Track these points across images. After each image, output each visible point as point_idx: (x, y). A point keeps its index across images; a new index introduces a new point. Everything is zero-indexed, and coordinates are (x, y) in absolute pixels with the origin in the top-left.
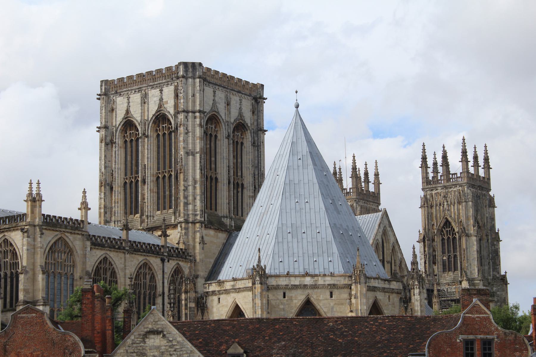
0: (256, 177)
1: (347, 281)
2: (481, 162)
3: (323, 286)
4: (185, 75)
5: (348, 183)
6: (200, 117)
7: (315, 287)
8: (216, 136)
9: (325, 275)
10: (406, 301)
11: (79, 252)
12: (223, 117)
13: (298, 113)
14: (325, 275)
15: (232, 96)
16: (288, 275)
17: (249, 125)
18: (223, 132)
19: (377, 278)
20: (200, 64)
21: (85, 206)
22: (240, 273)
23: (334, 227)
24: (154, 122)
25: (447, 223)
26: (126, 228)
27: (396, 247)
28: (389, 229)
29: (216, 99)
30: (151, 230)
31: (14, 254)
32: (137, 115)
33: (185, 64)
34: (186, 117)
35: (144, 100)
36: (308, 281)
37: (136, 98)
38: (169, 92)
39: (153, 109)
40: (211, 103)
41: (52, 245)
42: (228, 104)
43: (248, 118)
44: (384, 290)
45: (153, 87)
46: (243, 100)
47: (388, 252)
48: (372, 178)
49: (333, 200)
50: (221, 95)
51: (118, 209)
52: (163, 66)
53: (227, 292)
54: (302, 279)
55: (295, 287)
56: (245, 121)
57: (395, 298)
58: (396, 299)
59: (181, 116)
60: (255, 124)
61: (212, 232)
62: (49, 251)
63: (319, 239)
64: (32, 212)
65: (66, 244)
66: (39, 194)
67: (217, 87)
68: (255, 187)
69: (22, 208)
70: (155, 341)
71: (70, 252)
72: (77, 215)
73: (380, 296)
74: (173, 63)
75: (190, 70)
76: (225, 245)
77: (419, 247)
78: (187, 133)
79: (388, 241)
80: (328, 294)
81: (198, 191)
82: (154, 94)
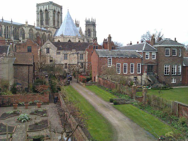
1: (75, 37)
2: (94, 20)
5: (75, 22)
7: (70, 38)
10: (84, 40)
13: (68, 11)
18: (56, 13)
21: (35, 24)
22: (59, 35)
23: (73, 29)
25: (89, 29)
26: (41, 27)
30: (45, 28)
31: (24, 31)
32: (42, 9)
36: (70, 37)
37: (42, 7)
38: (47, 6)
39: (45, 9)
44: (81, 39)
47: (81, 33)
48: (78, 22)
50: (56, 7)
51: (40, 24)
52: (47, 2)
53: (57, 38)
57: (82, 40)
59: (50, 10)
61: (54, 29)
65: (32, 30)
69: (25, 23)
70: (48, 45)
72: (33, 25)
73: (80, 40)
74: (48, 2)
77: (85, 33)
81: (52, 22)
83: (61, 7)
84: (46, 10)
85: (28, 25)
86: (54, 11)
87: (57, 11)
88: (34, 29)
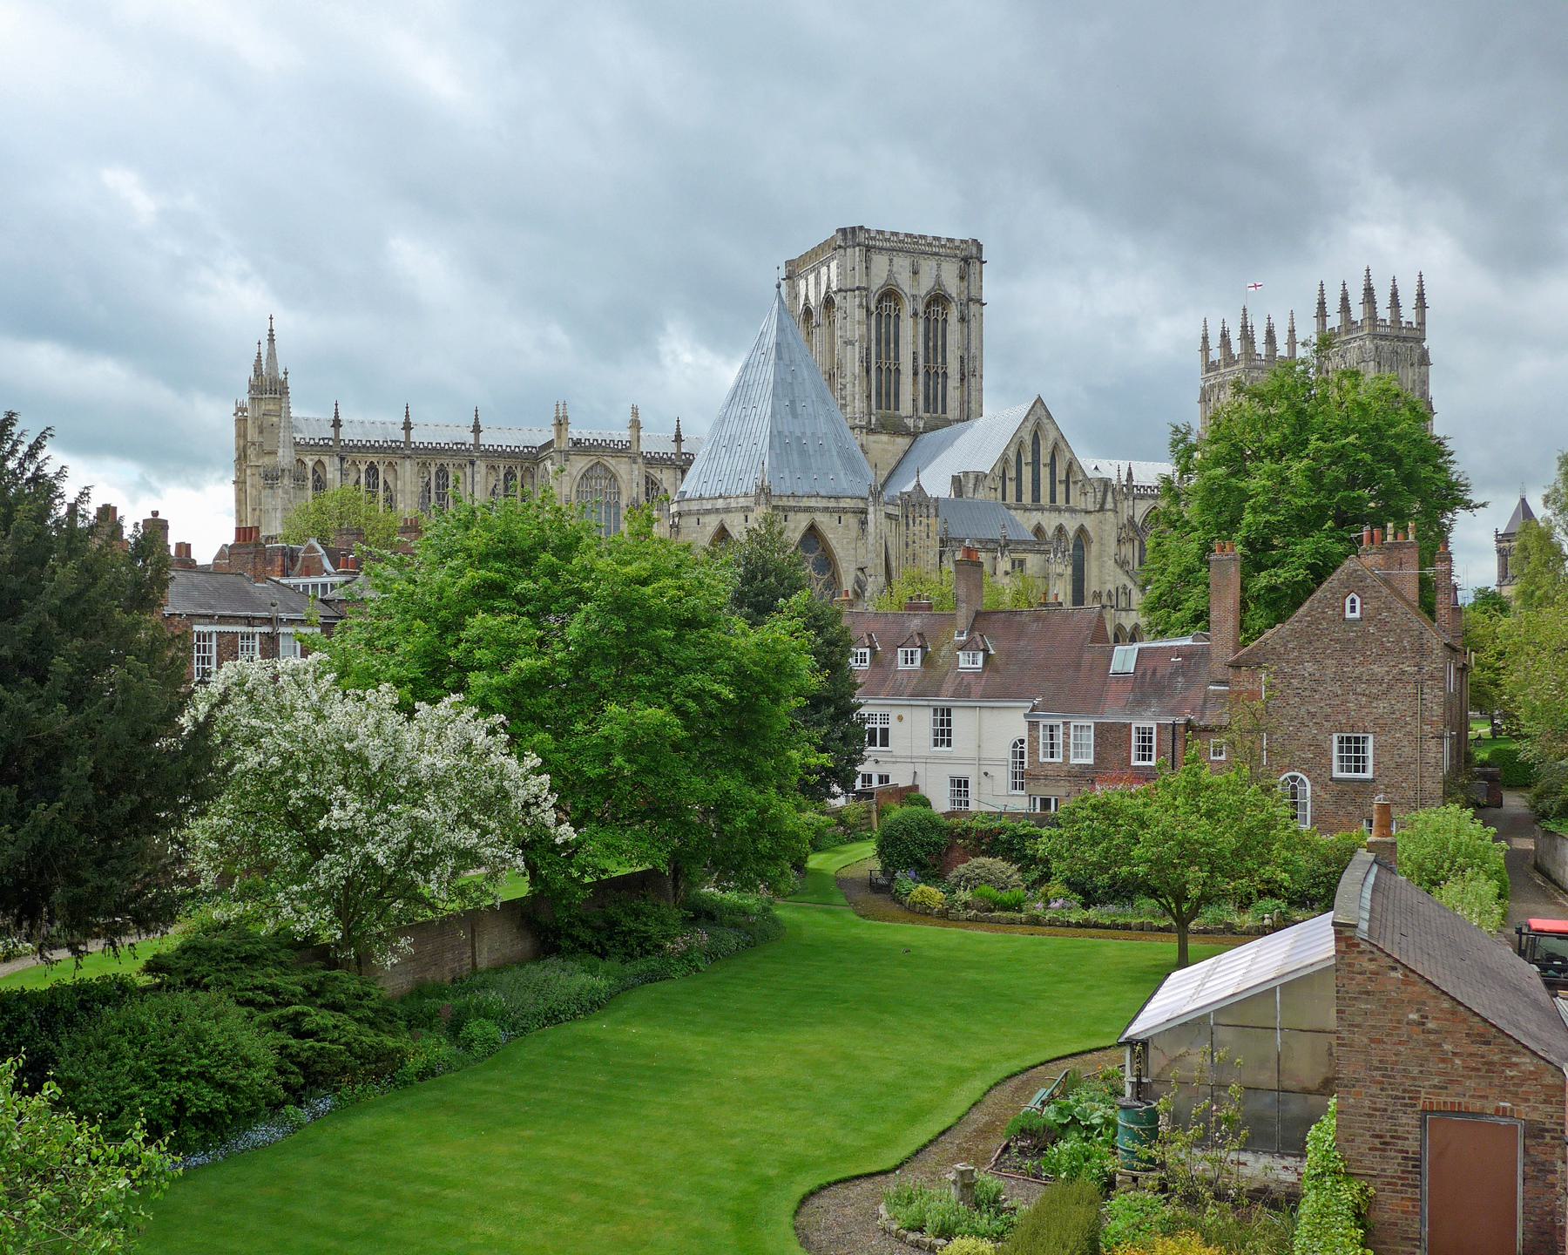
0: (966, 361)
3: (737, 510)
4: (842, 244)
6: (861, 296)
7: (727, 510)
8: (898, 316)
9: (738, 497)
11: (625, 477)
12: (907, 290)
14: (738, 497)
15: (922, 262)
16: (701, 498)
17: (954, 295)
19: (818, 495)
20: (861, 228)
23: (776, 436)
24: (826, 307)
27: (1062, 445)
28: (1046, 421)
29: (894, 269)
33: (843, 231)
34: (845, 298)
35: (817, 283)
36: (720, 503)
37: (812, 278)
40: (885, 275)
41: (587, 470)
42: (915, 273)
43: (952, 286)
44: (826, 509)
45: (822, 263)
46: (945, 266)
49: (792, 402)
50: (902, 264)
54: (715, 501)
55: (708, 512)
56: (945, 291)
58: (851, 520)
60: (966, 292)
62: (582, 478)
63: (753, 453)
64: (559, 437)
65: (606, 469)
66: (566, 418)
67: (895, 253)
68: (963, 374)
71: (613, 477)
72: (625, 435)
75: (849, 236)
76: (906, 453)
78: (845, 318)
79: (1046, 438)
80: (744, 518)
82: (824, 270)
83: (969, 257)
84: (829, 302)
85: (564, 446)
86: (890, 294)
87: (915, 289)
88: (621, 467)
